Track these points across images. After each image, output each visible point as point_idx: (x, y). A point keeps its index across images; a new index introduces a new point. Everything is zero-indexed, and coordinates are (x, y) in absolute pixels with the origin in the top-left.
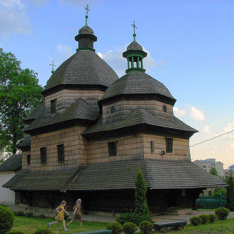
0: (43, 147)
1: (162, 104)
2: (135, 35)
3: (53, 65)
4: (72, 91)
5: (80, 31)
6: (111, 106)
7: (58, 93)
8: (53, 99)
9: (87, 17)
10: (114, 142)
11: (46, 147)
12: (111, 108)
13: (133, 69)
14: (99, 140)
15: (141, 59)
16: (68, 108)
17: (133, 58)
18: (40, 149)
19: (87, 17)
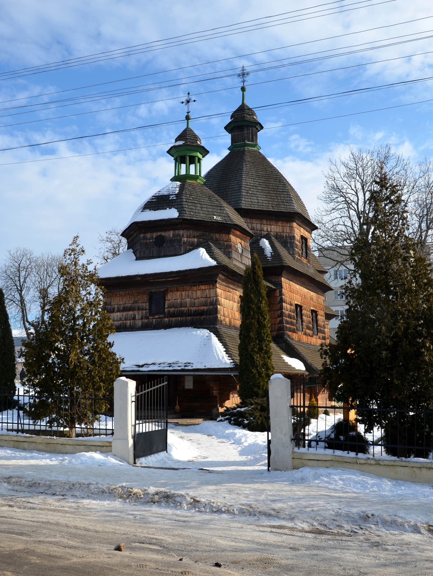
1: (155, 235)
9: (243, 89)
19: (243, 89)
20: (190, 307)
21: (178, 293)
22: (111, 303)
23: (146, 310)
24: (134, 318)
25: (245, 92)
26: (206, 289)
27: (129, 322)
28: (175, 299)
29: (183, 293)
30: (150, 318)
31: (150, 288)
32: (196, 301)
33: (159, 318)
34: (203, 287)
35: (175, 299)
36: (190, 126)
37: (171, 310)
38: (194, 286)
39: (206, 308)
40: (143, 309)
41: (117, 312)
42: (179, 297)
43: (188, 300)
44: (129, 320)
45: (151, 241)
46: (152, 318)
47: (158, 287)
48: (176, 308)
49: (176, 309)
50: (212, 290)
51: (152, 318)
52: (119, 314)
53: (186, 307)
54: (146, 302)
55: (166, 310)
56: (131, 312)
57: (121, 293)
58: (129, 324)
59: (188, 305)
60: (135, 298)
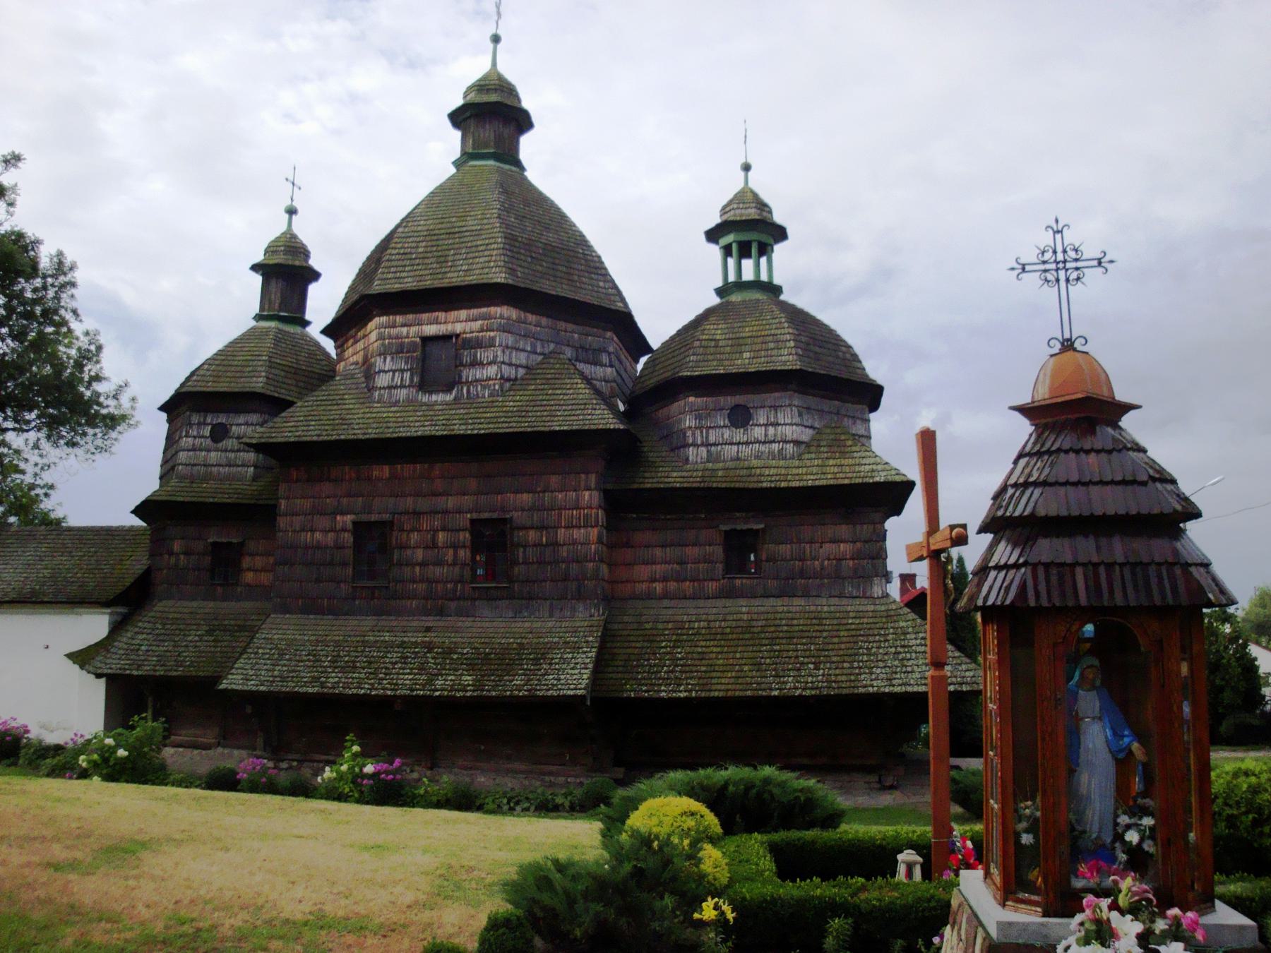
0: (364, 518)
2: (747, 168)
3: (293, 184)
4: (531, 318)
5: (481, 86)
6: (729, 401)
7: (463, 314)
8: (431, 330)
9: (496, 39)
10: (757, 531)
11: (392, 523)
12: (732, 409)
13: (740, 285)
14: (674, 516)
15: (764, 250)
16: (516, 379)
17: (735, 247)
18: (350, 526)
19: (496, 39)
25: (499, 46)
36: (751, 185)
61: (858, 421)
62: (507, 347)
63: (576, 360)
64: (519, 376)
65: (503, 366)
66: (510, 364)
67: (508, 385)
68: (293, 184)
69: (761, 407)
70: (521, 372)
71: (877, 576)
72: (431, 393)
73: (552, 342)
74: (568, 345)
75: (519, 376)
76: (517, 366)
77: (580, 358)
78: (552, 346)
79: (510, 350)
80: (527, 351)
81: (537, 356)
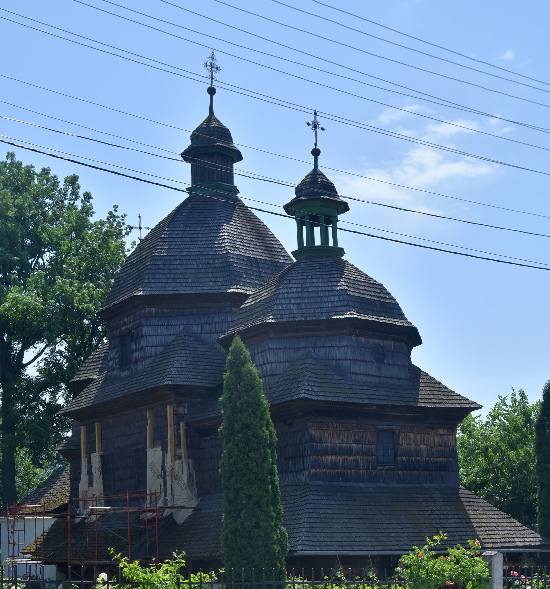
3: (140, 228)
15: (331, 220)
16: (156, 355)
20: (427, 457)
21: (412, 435)
22: (321, 439)
23: (372, 455)
24: (357, 467)
26: (444, 435)
27: (349, 471)
28: (408, 444)
29: (418, 436)
30: (378, 468)
31: (377, 423)
32: (433, 449)
33: (391, 470)
34: (441, 431)
35: (408, 444)
37: (404, 458)
38: (432, 429)
39: (445, 459)
40: (368, 455)
41: (332, 455)
42: (413, 442)
43: (423, 447)
44: (351, 469)
45: (367, 350)
46: (381, 468)
47: (387, 423)
48: (410, 457)
49: (411, 458)
50: (451, 436)
51: (381, 468)
52: (334, 457)
53: (422, 457)
54: (372, 444)
55: (399, 457)
56: (352, 458)
57: (335, 425)
58: (349, 476)
59: (425, 455)
60: (355, 435)
61: (336, 349)
62: (149, 336)
63: (202, 333)
64: (158, 353)
65: (146, 348)
66: (152, 346)
67: (151, 360)
68: (140, 228)
69: (258, 353)
70: (160, 349)
71: (304, 469)
72: (123, 371)
73: (181, 324)
74: (196, 324)
75: (158, 353)
76: (156, 346)
77: (204, 331)
78: (181, 327)
79: (152, 337)
80: (163, 335)
81: (171, 336)
